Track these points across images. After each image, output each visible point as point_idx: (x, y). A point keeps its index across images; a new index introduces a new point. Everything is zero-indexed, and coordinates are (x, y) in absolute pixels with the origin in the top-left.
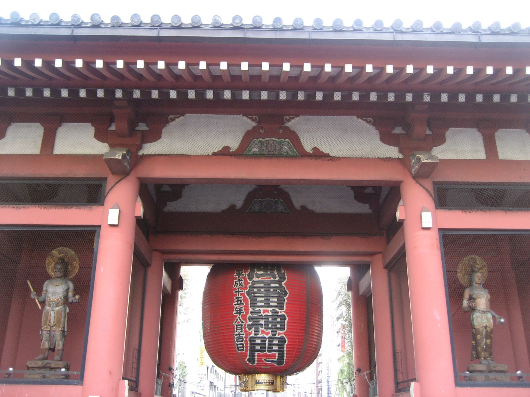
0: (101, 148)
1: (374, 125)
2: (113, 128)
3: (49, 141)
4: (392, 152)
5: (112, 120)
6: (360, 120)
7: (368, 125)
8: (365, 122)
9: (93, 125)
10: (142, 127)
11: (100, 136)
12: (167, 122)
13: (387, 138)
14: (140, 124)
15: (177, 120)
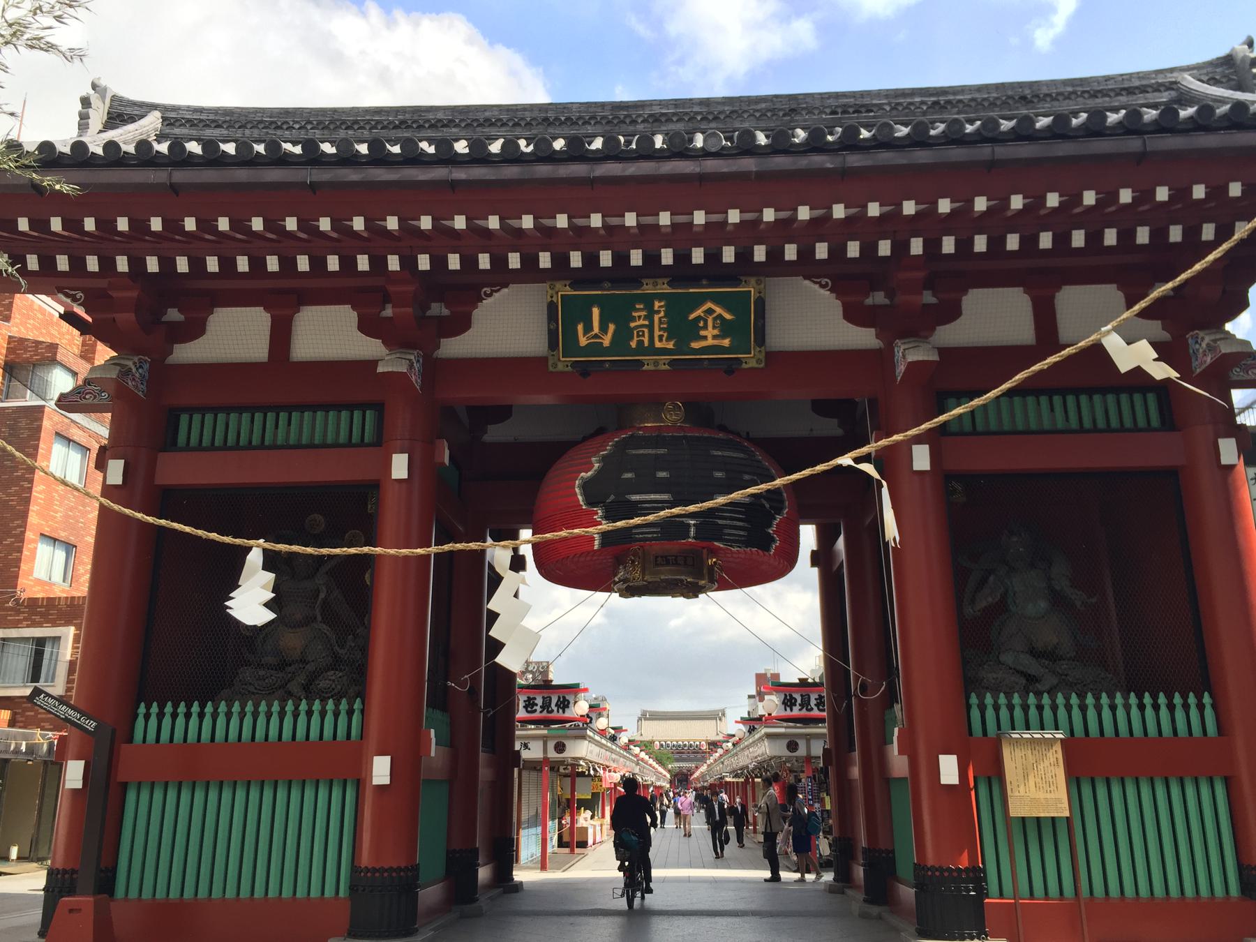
0: (369, 348)
1: (831, 290)
2: (388, 312)
3: (281, 335)
4: (864, 338)
5: (386, 299)
6: (807, 282)
7: (822, 291)
8: (817, 286)
9: (354, 308)
10: (438, 309)
11: (368, 326)
12: (481, 300)
13: (854, 315)
14: (433, 305)
15: (496, 295)
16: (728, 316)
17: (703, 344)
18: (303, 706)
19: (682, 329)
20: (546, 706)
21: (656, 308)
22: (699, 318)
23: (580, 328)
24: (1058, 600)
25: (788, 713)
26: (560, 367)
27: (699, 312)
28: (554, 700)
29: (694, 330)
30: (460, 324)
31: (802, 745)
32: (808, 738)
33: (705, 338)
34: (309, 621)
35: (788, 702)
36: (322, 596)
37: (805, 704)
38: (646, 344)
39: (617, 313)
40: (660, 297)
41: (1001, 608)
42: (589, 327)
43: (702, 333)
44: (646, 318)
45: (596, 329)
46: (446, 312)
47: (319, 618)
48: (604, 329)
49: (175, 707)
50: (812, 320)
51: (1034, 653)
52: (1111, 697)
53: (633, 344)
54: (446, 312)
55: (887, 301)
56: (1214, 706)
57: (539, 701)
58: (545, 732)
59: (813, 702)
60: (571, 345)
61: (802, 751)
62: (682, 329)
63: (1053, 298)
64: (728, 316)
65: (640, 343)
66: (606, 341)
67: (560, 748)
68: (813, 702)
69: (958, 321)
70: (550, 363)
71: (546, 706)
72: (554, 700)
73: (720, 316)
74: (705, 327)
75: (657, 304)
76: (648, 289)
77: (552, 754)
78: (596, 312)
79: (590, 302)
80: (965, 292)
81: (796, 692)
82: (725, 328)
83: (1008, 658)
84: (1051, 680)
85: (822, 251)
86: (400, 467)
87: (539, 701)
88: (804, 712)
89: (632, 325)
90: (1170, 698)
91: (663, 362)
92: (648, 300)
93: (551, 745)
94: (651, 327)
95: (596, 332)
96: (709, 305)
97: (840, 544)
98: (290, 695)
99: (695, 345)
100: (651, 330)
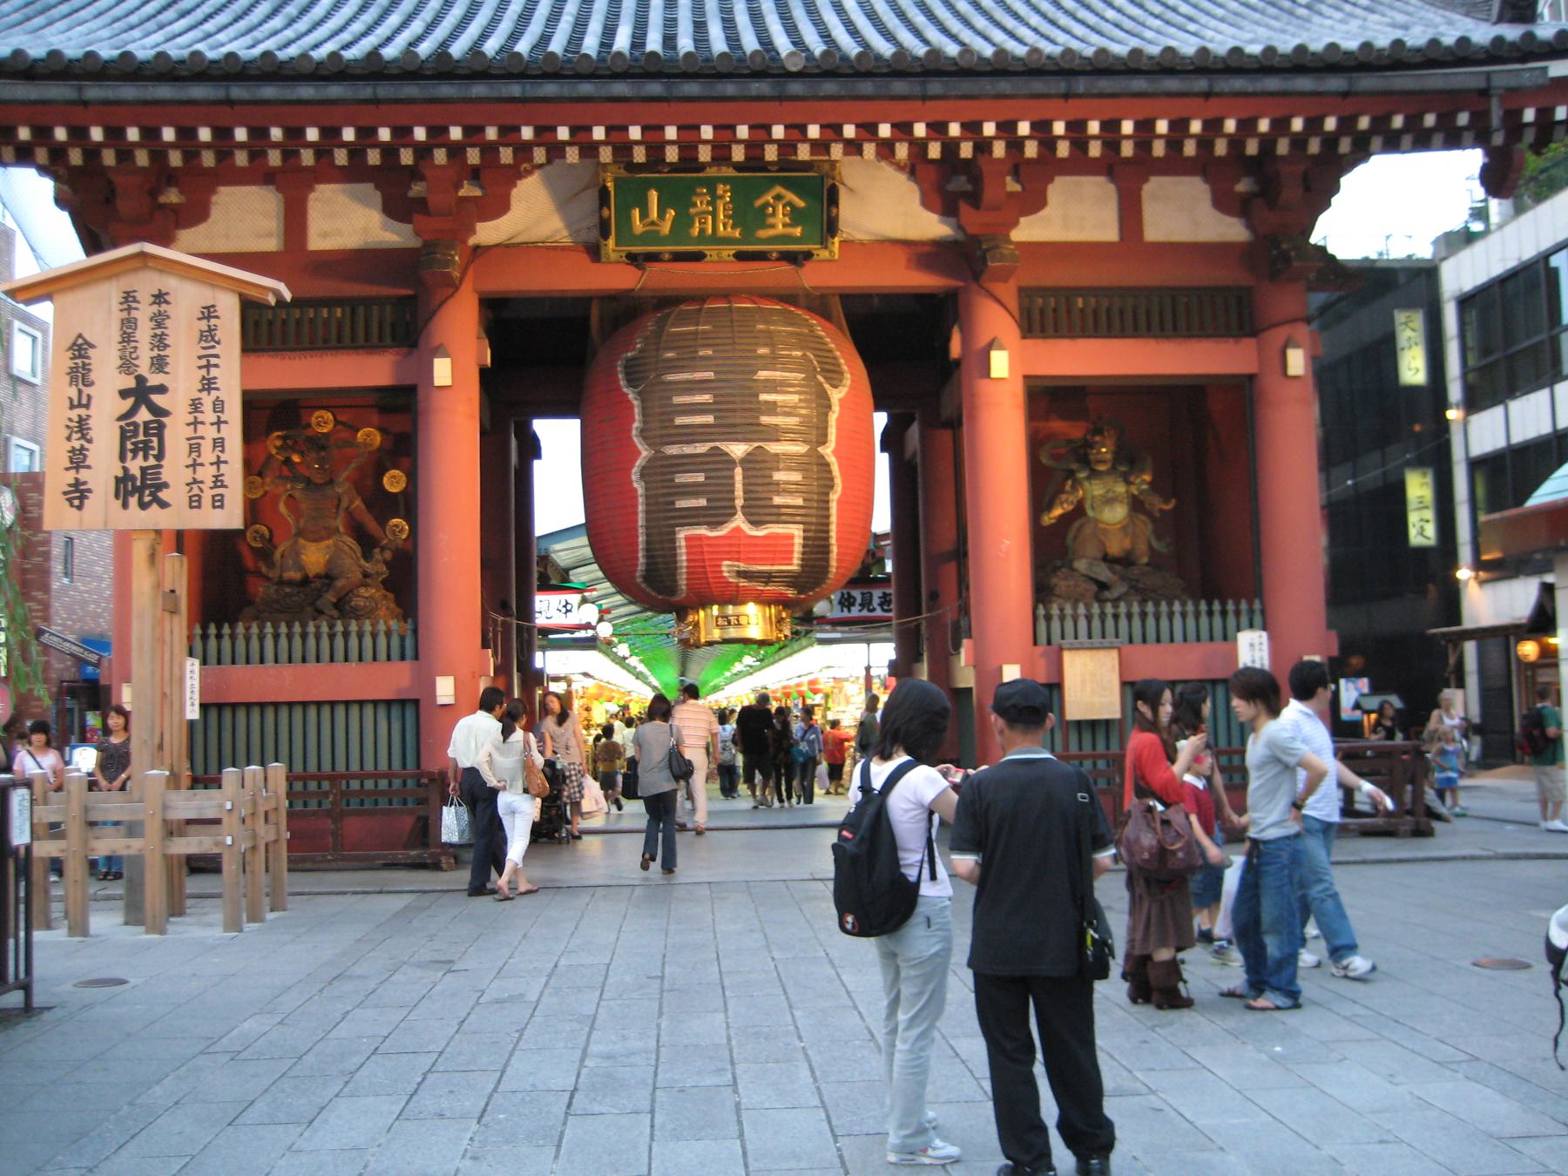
9: (377, 187)
11: (396, 208)
12: (520, 176)
16: (801, 203)
17: (771, 232)
18: (339, 628)
19: (749, 216)
21: (720, 192)
22: (767, 205)
23: (636, 213)
24: (1136, 505)
25: (846, 614)
26: (614, 256)
27: (769, 198)
29: (762, 217)
30: (498, 206)
33: (773, 226)
34: (334, 531)
36: (344, 504)
37: (866, 603)
38: (710, 231)
39: (677, 198)
40: (725, 180)
41: (1079, 511)
42: (644, 214)
43: (771, 220)
44: (708, 203)
45: (654, 214)
46: (477, 193)
47: (342, 529)
48: (661, 214)
49: (219, 628)
50: (885, 209)
51: (1106, 558)
52: (1170, 605)
53: (696, 232)
54: (477, 193)
55: (969, 187)
56: (1263, 612)
59: (876, 601)
60: (626, 234)
62: (749, 216)
63: (1140, 189)
64: (801, 203)
65: (702, 231)
66: (666, 228)
68: (876, 601)
69: (1042, 213)
70: (603, 253)
73: (790, 204)
74: (774, 214)
75: (720, 189)
76: (712, 172)
78: (653, 196)
79: (647, 185)
80: (1051, 180)
82: (796, 216)
83: (1081, 565)
84: (1120, 589)
85: (902, 151)
86: (442, 372)
88: (865, 613)
89: (692, 211)
90: (1223, 604)
91: (728, 252)
92: (711, 184)
94: (714, 214)
95: (652, 216)
96: (779, 190)
97: (914, 431)
98: (320, 612)
99: (762, 234)
100: (714, 216)
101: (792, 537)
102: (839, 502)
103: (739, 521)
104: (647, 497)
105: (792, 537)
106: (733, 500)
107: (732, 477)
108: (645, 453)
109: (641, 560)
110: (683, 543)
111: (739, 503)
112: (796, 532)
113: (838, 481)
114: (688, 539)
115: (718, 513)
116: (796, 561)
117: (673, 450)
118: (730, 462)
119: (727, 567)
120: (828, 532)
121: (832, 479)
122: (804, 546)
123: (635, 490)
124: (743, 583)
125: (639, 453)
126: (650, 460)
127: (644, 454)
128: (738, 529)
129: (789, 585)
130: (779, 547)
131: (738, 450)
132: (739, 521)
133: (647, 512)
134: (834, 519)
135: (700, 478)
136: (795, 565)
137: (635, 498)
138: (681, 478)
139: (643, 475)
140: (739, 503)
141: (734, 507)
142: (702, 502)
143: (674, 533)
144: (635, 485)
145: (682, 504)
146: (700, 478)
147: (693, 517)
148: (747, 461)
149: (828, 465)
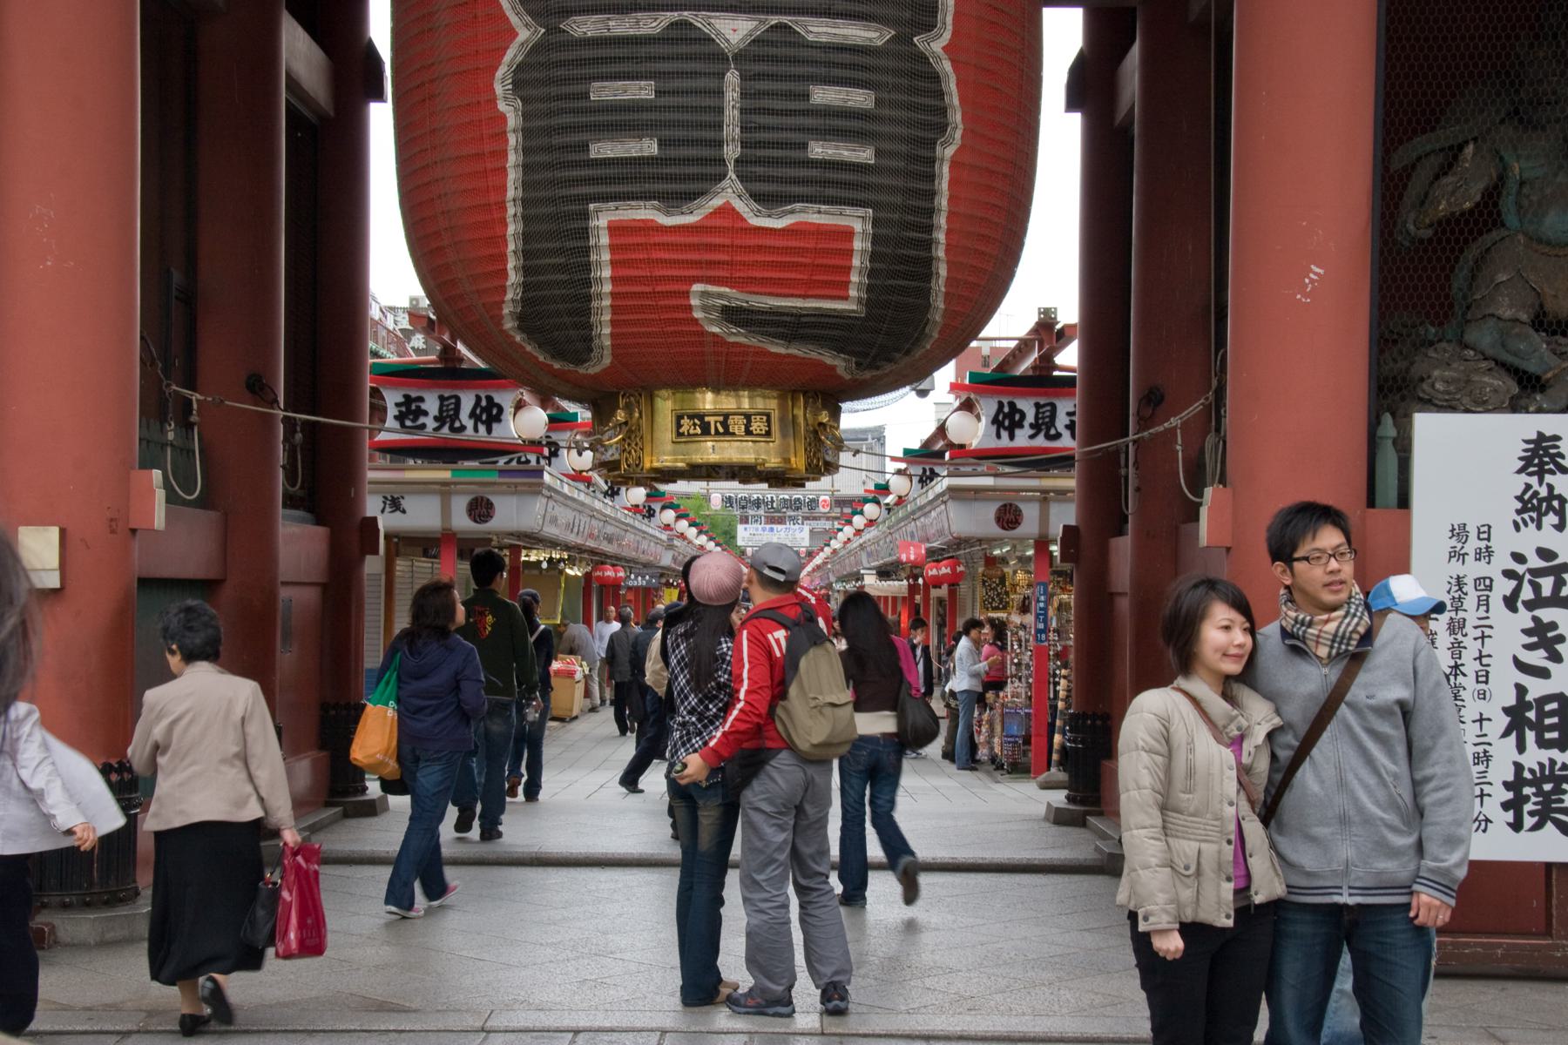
20: (448, 415)
25: (1004, 442)
28: (467, 402)
31: (1030, 512)
32: (1045, 497)
35: (1007, 421)
37: (1044, 424)
57: (431, 405)
58: (444, 474)
59: (1062, 421)
61: (1030, 525)
67: (481, 509)
71: (448, 415)
72: (467, 402)
77: (461, 521)
81: (1023, 395)
87: (431, 405)
88: (1040, 441)
93: (460, 505)
101: (848, 234)
102: (955, 164)
103: (730, 194)
104: (527, 133)
105: (848, 234)
106: (719, 144)
107: (720, 93)
108: (525, 34)
109: (513, 278)
110: (605, 240)
111: (731, 152)
112: (857, 222)
113: (956, 117)
114: (614, 229)
115: (680, 178)
116: (853, 293)
117: (586, 27)
118: (714, 56)
119: (704, 299)
120: (929, 229)
121: (943, 111)
122: (874, 257)
123: (503, 118)
124: (737, 336)
125: (514, 34)
126: (536, 49)
127: (523, 34)
128: (727, 211)
129: (839, 347)
130: (820, 258)
131: (733, 30)
132: (730, 194)
133: (527, 168)
134: (943, 202)
135: (643, 91)
136: (850, 303)
137: (502, 136)
138: (604, 92)
139: (519, 83)
140: (731, 152)
141: (721, 161)
142: (649, 147)
143: (585, 216)
144: (502, 106)
145: (603, 149)
146: (643, 91)
147: (627, 180)
148: (751, 56)
149: (935, 78)
